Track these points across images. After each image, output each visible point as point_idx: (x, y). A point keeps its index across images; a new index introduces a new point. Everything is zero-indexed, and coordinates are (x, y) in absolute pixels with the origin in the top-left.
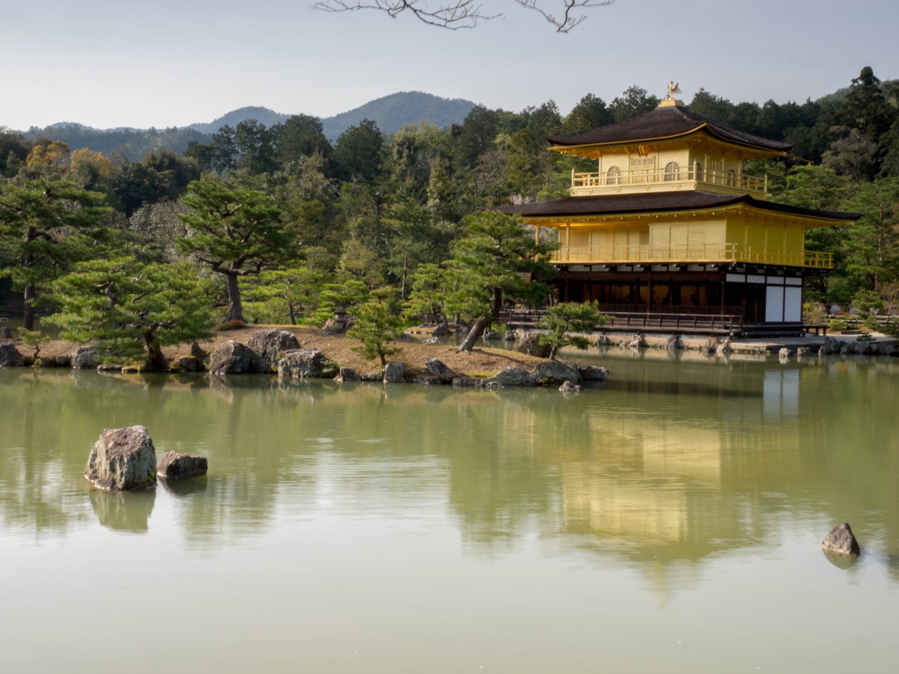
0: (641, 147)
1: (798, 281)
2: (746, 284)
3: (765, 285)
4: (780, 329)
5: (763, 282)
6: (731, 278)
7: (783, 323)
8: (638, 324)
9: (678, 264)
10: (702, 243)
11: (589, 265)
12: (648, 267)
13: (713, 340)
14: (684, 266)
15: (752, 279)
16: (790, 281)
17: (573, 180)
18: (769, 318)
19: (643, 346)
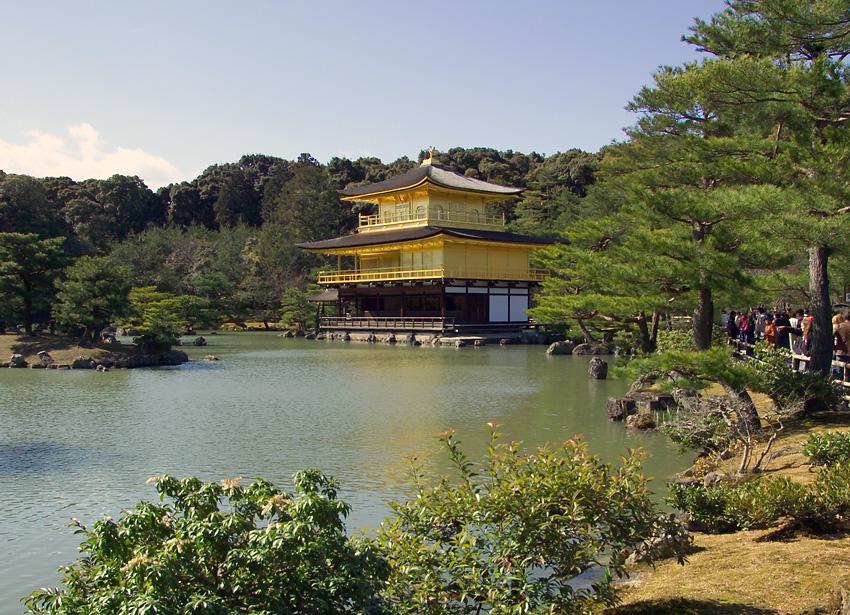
0: (402, 197)
1: (526, 291)
2: (467, 295)
3: (488, 295)
4: (497, 327)
5: (486, 292)
6: (448, 290)
7: (509, 322)
8: (391, 326)
9: (413, 281)
10: (428, 266)
11: (368, 283)
12: (399, 284)
13: (433, 336)
14: (419, 283)
15: (471, 290)
16: (512, 291)
17: (360, 221)
18: (491, 320)
19: (393, 341)
